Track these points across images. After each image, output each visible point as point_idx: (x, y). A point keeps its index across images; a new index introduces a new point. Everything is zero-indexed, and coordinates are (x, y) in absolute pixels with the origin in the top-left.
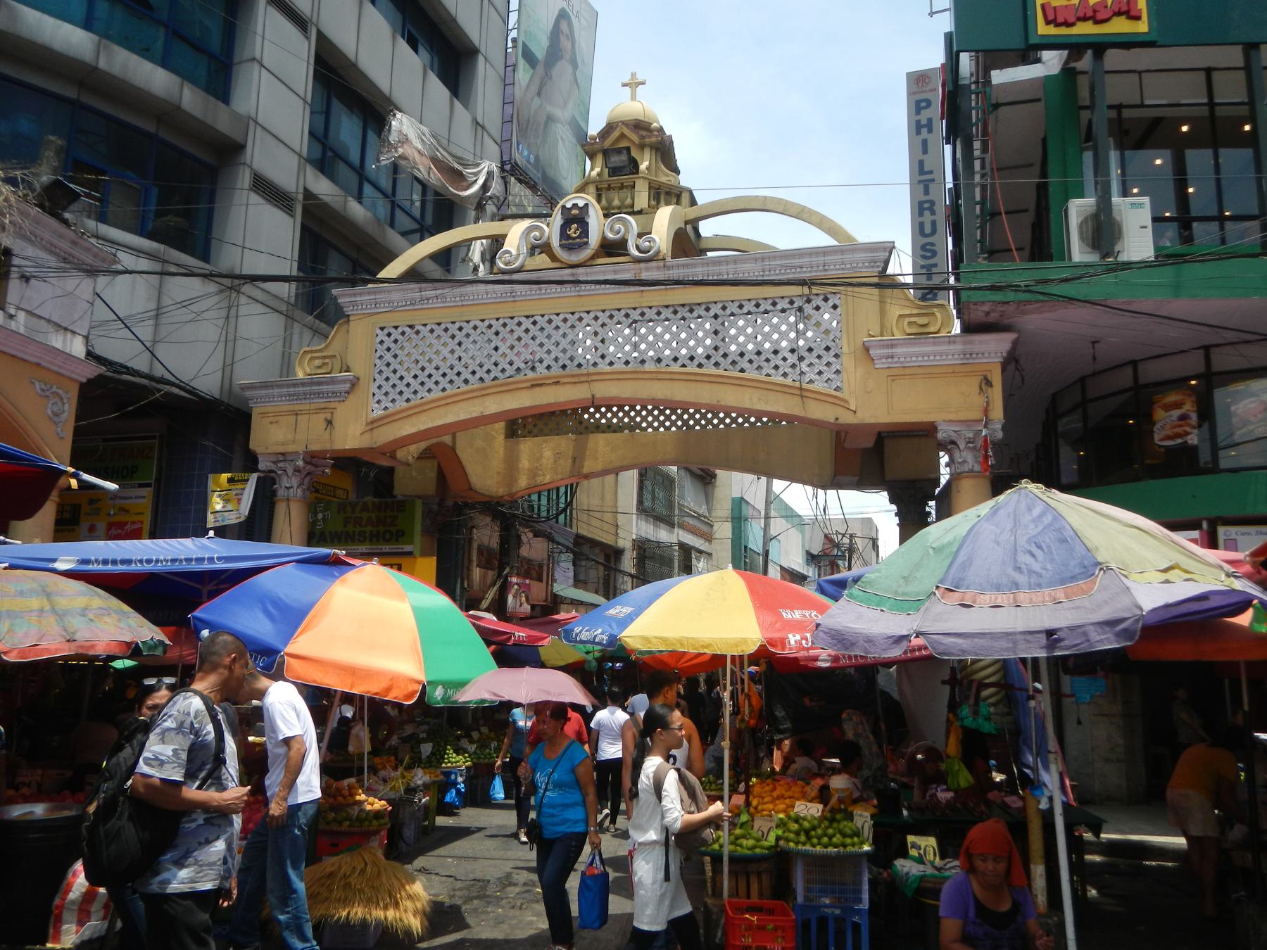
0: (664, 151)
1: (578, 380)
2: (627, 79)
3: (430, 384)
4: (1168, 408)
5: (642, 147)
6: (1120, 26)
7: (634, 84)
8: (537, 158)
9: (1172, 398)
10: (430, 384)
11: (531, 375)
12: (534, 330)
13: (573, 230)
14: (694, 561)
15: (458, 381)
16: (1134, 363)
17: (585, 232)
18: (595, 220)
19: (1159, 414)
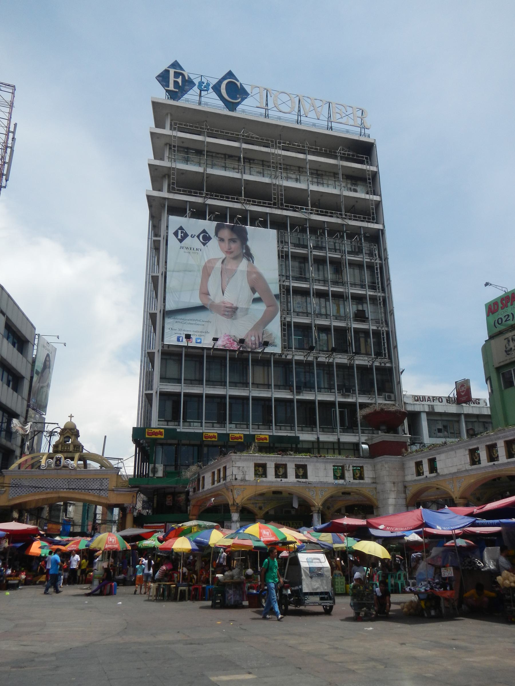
0: (77, 434)
1: (56, 493)
2: (70, 415)
3: (23, 492)
4: (169, 498)
5: (72, 435)
6: (159, 436)
7: (71, 416)
8: (37, 401)
9: (169, 496)
10: (23, 492)
11: (46, 491)
12: (47, 482)
13: (58, 462)
14: (68, 507)
15: (30, 492)
16: (164, 489)
17: (60, 463)
18: (63, 460)
19: (167, 499)
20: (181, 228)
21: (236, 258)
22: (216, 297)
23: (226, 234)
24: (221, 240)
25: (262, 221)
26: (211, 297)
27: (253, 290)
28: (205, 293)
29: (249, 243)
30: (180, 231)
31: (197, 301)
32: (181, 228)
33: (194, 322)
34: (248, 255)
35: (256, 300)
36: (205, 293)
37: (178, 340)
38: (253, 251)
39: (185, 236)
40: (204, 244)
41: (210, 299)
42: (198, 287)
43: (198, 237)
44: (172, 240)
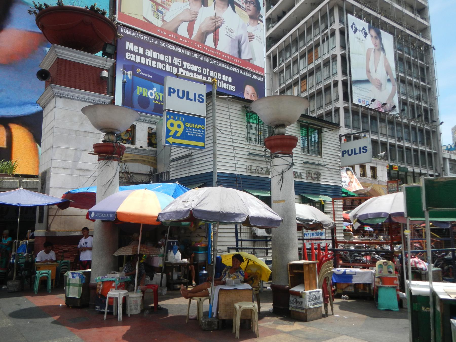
20: (354, 24)
21: (379, 50)
22: (374, 76)
23: (373, 32)
24: (372, 36)
25: (385, 27)
26: (371, 74)
27: (388, 74)
28: (368, 72)
29: (383, 41)
30: (353, 26)
31: (365, 77)
32: (354, 24)
33: (365, 90)
34: (383, 49)
35: (389, 80)
36: (368, 72)
37: (359, 101)
38: (385, 47)
39: (356, 30)
40: (365, 37)
41: (371, 76)
42: (365, 66)
43: (362, 31)
44: (351, 31)
